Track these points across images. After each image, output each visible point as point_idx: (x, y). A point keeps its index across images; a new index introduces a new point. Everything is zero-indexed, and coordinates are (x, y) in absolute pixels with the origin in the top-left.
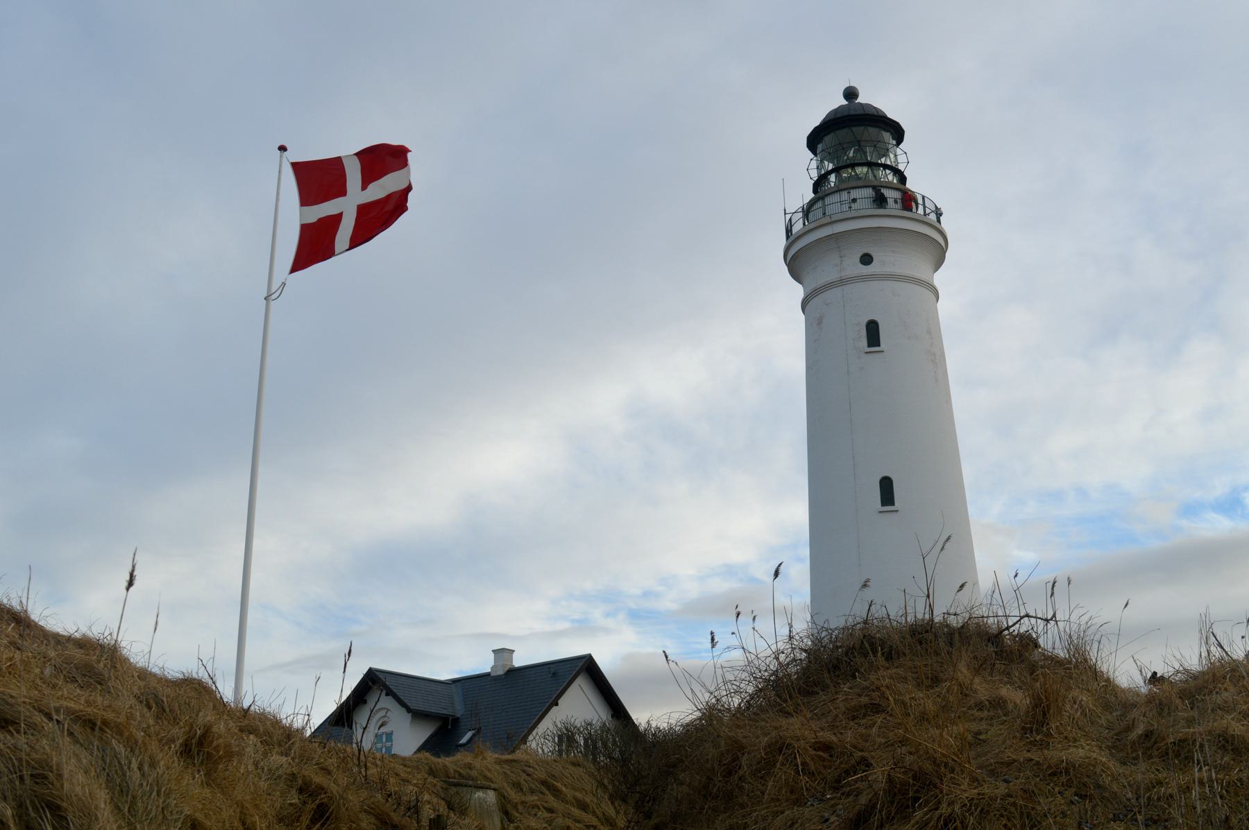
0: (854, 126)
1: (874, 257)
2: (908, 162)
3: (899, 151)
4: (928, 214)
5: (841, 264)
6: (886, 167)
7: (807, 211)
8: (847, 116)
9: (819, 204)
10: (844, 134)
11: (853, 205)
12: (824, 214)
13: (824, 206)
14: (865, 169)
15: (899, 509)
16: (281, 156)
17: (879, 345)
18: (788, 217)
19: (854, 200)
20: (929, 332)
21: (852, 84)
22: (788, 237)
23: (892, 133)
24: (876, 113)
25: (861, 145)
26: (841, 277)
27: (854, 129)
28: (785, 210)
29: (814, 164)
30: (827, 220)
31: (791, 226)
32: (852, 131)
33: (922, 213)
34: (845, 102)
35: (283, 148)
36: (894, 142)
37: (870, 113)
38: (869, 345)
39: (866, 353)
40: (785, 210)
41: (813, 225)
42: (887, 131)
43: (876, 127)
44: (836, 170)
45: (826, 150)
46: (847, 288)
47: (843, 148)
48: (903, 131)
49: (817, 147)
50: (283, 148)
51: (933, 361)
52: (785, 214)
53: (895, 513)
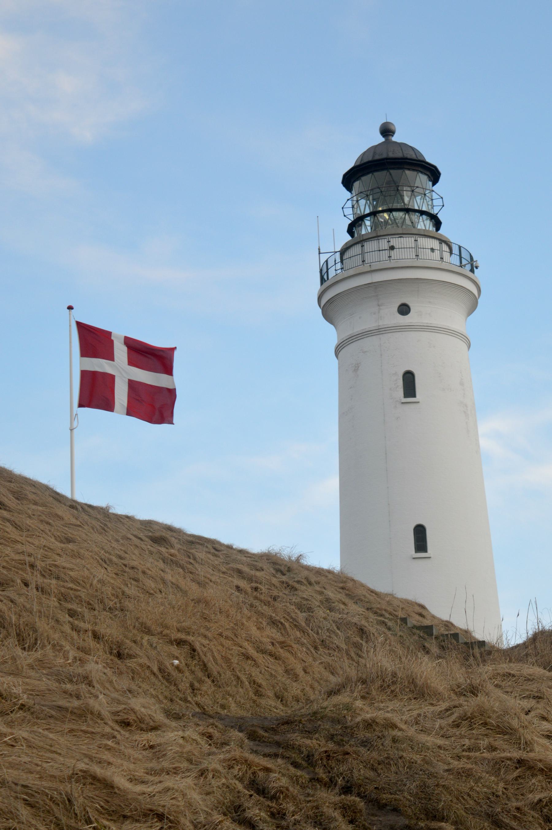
0: (393, 169)
1: (411, 308)
2: (443, 206)
3: (435, 196)
4: (465, 266)
5: (379, 312)
6: (422, 213)
7: (343, 252)
8: (387, 159)
9: (357, 249)
10: (382, 176)
11: (393, 253)
12: (363, 261)
13: (363, 253)
14: (401, 214)
15: (432, 556)
16: (70, 314)
17: (414, 395)
18: (324, 258)
19: (392, 248)
20: (462, 384)
21: (388, 121)
22: (322, 280)
23: (429, 177)
24: (414, 157)
25: (399, 189)
26: (379, 326)
27: (392, 171)
28: (319, 249)
29: (349, 204)
30: (366, 268)
31: (328, 269)
32: (391, 174)
33: (458, 264)
34: (382, 139)
35: (70, 308)
36: (431, 183)
37: (409, 157)
38: (406, 395)
39: (402, 403)
40: (319, 249)
41: (351, 272)
42: (425, 174)
43: (414, 170)
44: (374, 214)
45: (365, 193)
46: (385, 338)
47: (381, 192)
48: (439, 174)
49: (352, 185)
50: (70, 308)
51: (465, 412)
52: (319, 253)
53: (427, 560)
